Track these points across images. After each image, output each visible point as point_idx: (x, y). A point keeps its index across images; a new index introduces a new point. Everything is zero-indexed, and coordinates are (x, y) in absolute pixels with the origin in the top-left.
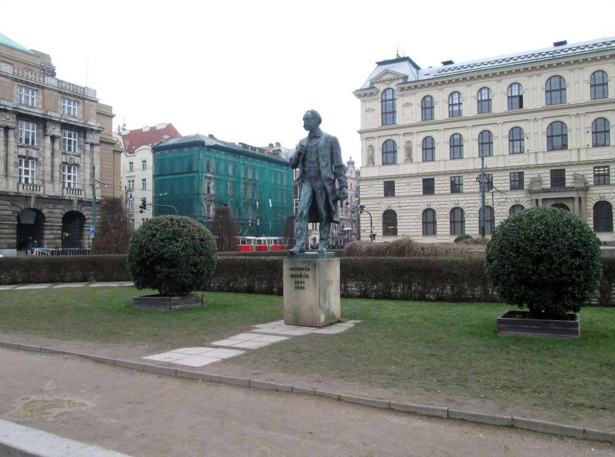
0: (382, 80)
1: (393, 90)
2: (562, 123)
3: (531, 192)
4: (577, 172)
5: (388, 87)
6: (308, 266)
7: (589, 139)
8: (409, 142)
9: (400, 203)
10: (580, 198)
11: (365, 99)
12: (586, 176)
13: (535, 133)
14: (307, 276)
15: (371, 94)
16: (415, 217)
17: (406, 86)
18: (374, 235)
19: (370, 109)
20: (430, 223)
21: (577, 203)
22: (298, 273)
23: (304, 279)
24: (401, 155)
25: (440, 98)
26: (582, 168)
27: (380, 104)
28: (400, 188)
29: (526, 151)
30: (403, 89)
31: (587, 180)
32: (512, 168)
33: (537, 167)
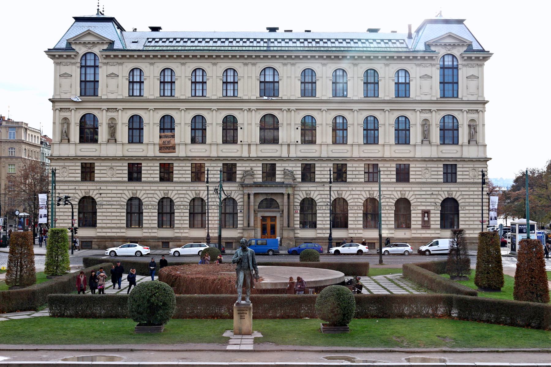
0: (82, 42)
3: (243, 185)
4: (287, 168)
5: (90, 51)
7: (297, 135)
8: (113, 119)
10: (289, 195)
11: (59, 61)
13: (248, 124)
15: (68, 56)
17: (112, 54)
19: (66, 73)
20: (167, 213)
21: (286, 197)
24: (103, 134)
25: (152, 72)
27: (79, 69)
28: (101, 172)
29: (239, 142)
30: (108, 57)
31: (296, 176)
32: (265, 158)
33: (249, 159)
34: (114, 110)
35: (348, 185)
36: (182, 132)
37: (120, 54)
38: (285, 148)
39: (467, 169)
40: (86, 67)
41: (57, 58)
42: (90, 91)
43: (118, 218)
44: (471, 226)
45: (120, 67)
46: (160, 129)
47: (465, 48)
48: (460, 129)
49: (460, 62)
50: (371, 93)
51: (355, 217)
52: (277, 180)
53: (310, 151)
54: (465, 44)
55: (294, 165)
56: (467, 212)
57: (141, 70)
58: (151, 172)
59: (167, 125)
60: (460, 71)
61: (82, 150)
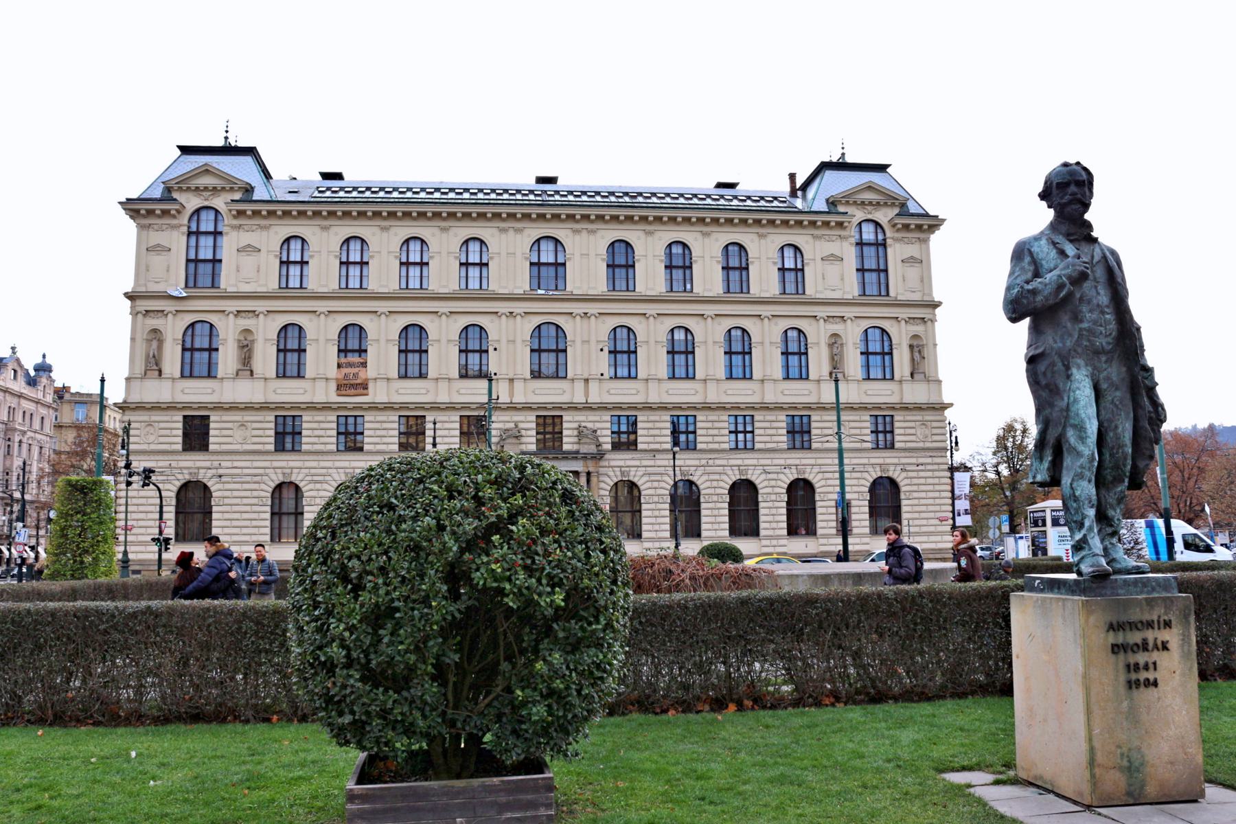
1: (217, 211)
2: (558, 327)
5: (206, 203)
6: (1166, 614)
7: (603, 363)
8: (247, 331)
9: (220, 466)
10: (589, 474)
12: (599, 433)
14: (1165, 647)
15: (165, 213)
16: (255, 501)
17: (249, 208)
18: (167, 541)
19: (158, 245)
22: (1135, 637)
23: (1155, 656)
24: (227, 359)
26: (593, 416)
27: (185, 238)
30: (241, 213)
31: (601, 440)
34: (251, 315)
35: (700, 456)
36: (382, 356)
37: (264, 208)
38: (580, 385)
39: (912, 424)
40: (198, 233)
41: (144, 217)
42: (204, 280)
43: (255, 523)
44: (924, 529)
45: (265, 233)
46: (340, 351)
47: (896, 211)
48: (895, 352)
49: (888, 234)
50: (734, 286)
51: (773, 513)
52: (566, 447)
53: (626, 392)
54: (897, 203)
55: (597, 418)
56: (916, 502)
57: (303, 240)
58: (319, 432)
59: (352, 344)
60: (889, 250)
61: (279, 391)
